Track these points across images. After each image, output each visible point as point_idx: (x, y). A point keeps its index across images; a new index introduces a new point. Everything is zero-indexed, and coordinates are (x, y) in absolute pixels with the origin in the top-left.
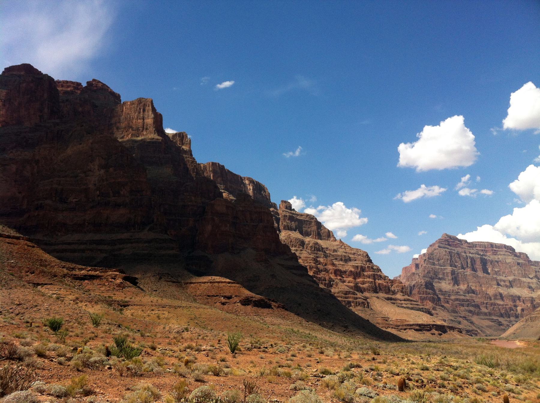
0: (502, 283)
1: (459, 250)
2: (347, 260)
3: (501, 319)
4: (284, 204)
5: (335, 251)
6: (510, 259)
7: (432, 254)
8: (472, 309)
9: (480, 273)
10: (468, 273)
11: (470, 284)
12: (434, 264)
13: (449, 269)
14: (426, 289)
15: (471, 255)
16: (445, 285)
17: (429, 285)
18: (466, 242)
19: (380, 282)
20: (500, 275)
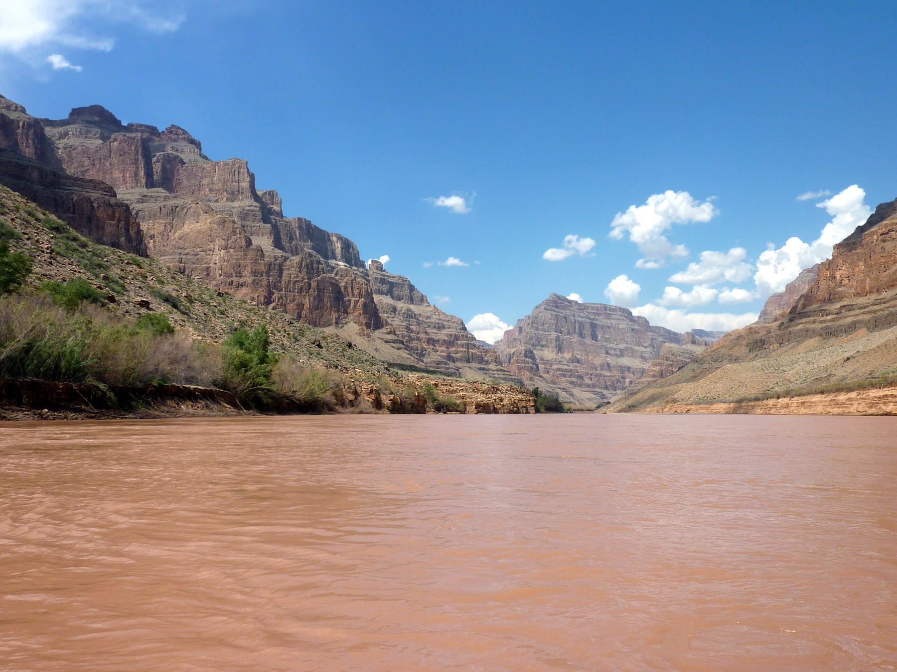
0: (612, 352)
1: (568, 312)
2: (441, 327)
3: (605, 392)
4: (375, 264)
5: (428, 317)
6: (623, 325)
7: (536, 317)
8: (574, 379)
9: (588, 341)
10: (574, 340)
11: (575, 352)
12: (537, 329)
13: (554, 335)
14: (526, 356)
15: (580, 319)
16: (548, 354)
17: (529, 354)
18: (576, 303)
19: (473, 351)
20: (610, 342)
